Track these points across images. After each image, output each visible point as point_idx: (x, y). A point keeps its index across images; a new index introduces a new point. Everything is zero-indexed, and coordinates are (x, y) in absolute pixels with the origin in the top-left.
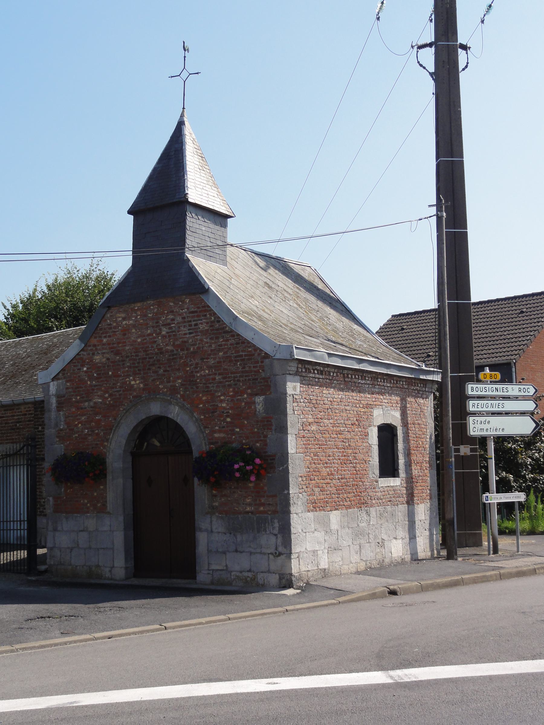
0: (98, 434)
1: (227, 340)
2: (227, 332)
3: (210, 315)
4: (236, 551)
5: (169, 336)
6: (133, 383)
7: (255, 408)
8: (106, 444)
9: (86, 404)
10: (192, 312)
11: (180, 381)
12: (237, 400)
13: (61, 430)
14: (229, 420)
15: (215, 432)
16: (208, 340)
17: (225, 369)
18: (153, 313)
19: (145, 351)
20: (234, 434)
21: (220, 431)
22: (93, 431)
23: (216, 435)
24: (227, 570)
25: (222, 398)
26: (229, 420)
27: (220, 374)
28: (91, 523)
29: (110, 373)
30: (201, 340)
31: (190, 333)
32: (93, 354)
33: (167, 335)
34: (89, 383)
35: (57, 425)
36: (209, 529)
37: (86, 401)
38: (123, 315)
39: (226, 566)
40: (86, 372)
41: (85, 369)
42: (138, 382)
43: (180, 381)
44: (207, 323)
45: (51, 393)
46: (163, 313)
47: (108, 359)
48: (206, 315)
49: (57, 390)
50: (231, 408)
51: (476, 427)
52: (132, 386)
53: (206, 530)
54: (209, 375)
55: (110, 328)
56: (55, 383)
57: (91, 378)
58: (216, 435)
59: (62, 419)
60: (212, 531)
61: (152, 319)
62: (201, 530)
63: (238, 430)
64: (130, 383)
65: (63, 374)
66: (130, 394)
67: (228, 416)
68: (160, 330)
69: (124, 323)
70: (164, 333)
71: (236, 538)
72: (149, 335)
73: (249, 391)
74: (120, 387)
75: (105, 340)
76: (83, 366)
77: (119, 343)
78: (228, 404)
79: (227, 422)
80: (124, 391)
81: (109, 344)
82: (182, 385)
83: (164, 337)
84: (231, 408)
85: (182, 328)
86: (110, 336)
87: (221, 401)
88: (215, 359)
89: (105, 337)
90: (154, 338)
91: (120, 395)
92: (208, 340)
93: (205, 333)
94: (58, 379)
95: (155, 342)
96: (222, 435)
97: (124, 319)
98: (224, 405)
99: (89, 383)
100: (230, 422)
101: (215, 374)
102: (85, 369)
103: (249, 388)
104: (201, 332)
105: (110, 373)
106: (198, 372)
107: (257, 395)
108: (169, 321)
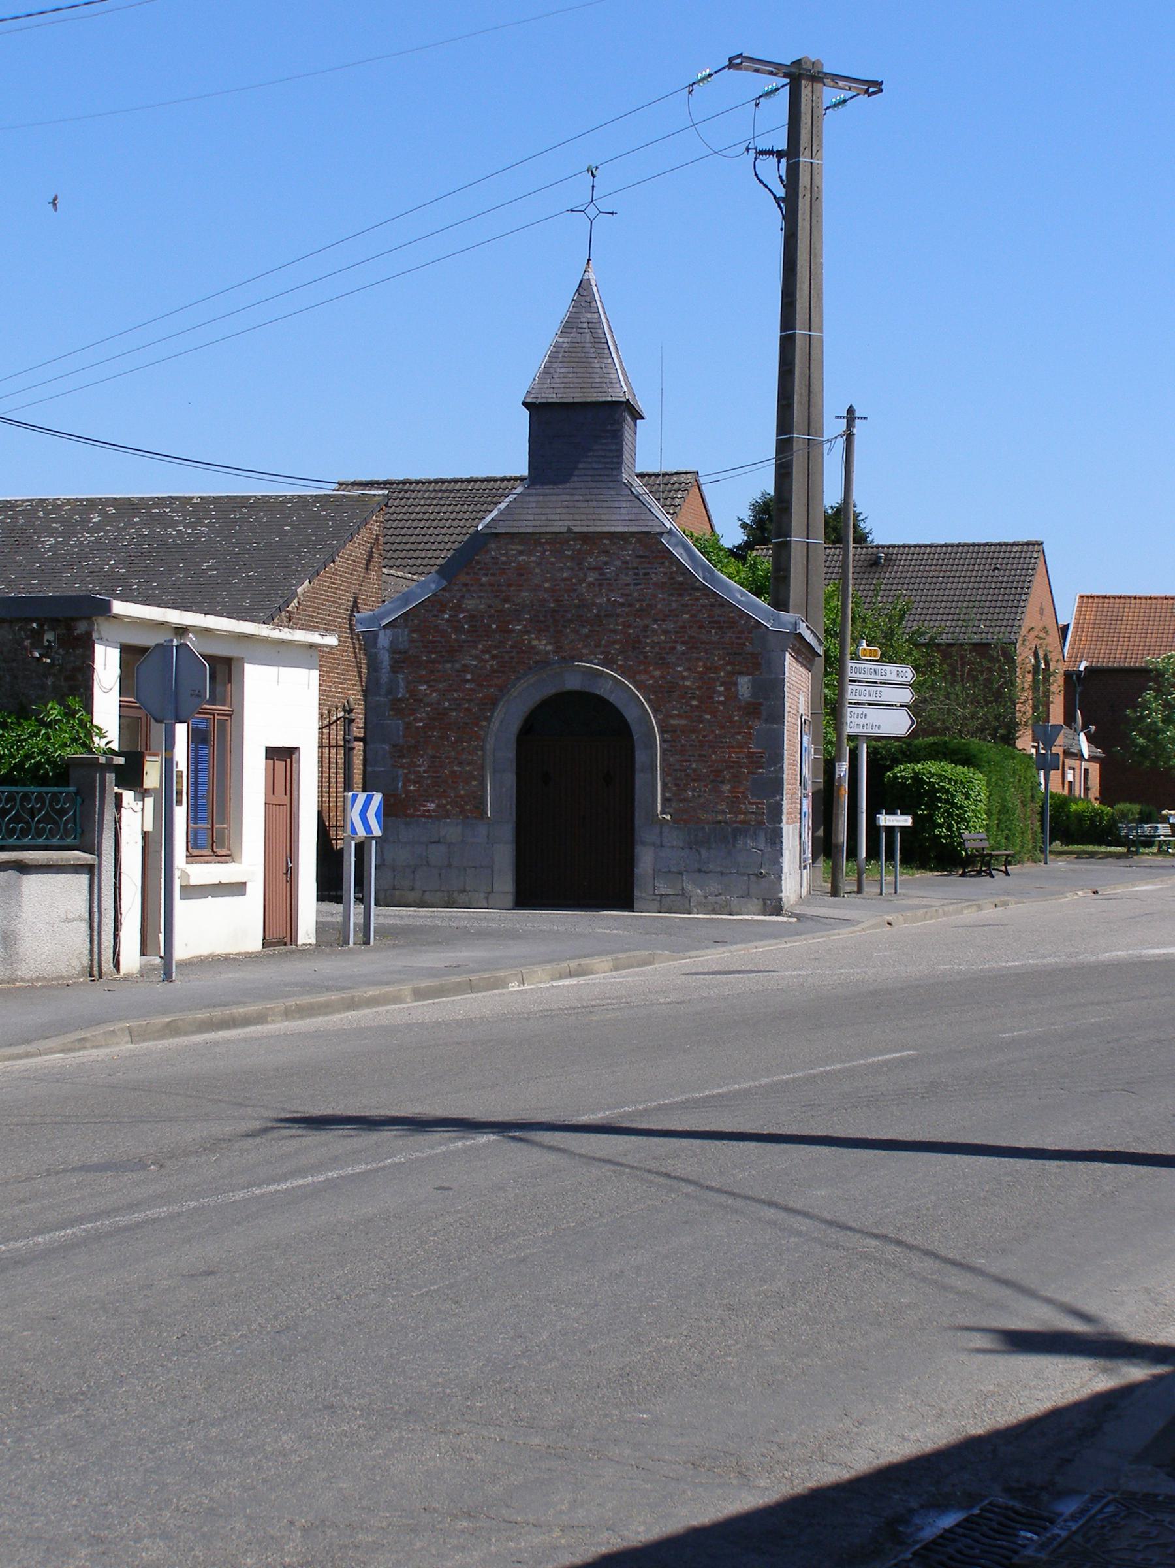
0: (468, 709)
1: (697, 600)
2: (697, 589)
3: (671, 564)
4: (700, 871)
5: (600, 585)
6: (535, 643)
7: (737, 691)
8: (485, 723)
9: (449, 666)
10: (641, 557)
11: (617, 647)
12: (709, 678)
13: (399, 700)
14: (694, 703)
15: (672, 717)
16: (666, 596)
17: (690, 637)
18: (574, 550)
19: (557, 601)
20: (701, 722)
21: (679, 716)
22: (459, 705)
23: (673, 722)
24: (683, 895)
25: (685, 674)
26: (694, 703)
27: (683, 643)
28: (452, 831)
29: (494, 626)
30: (655, 596)
31: (636, 584)
32: (463, 597)
33: (597, 583)
34: (453, 636)
35: (390, 692)
36: (658, 843)
37: (448, 662)
38: (520, 548)
39: (683, 889)
40: (447, 620)
41: (446, 616)
42: (544, 642)
43: (617, 647)
44: (665, 574)
45: (380, 645)
46: (590, 553)
47: (490, 606)
48: (662, 563)
49: (391, 642)
50: (699, 688)
51: (850, 729)
52: (533, 647)
53: (654, 844)
54: (665, 642)
55: (496, 563)
56: (389, 632)
57: (458, 629)
58: (673, 722)
59: (402, 684)
60: (662, 846)
61: (572, 558)
62: (643, 843)
63: (709, 717)
64: (530, 642)
65: (406, 620)
66: (529, 658)
67: (694, 698)
68: (585, 575)
69: (521, 558)
70: (590, 579)
71: (700, 853)
72: (564, 580)
73: (729, 668)
74: (512, 647)
75: (484, 579)
76: (444, 612)
77: (510, 585)
78: (693, 683)
79: (691, 706)
80: (518, 653)
81: (491, 585)
82: (621, 652)
83: (591, 584)
84: (699, 688)
85: (622, 576)
86: (493, 575)
87: (684, 678)
88: (675, 622)
89: (486, 575)
90: (575, 584)
91: (512, 658)
92: (666, 596)
93: (661, 586)
94: (395, 627)
95: (575, 590)
96: (683, 722)
97: (521, 553)
98: (688, 683)
99: (453, 636)
100: (697, 707)
101: (676, 642)
102: (446, 616)
103: (729, 663)
104: (655, 584)
105: (494, 626)
106: (647, 637)
107: (740, 673)
108: (600, 564)
